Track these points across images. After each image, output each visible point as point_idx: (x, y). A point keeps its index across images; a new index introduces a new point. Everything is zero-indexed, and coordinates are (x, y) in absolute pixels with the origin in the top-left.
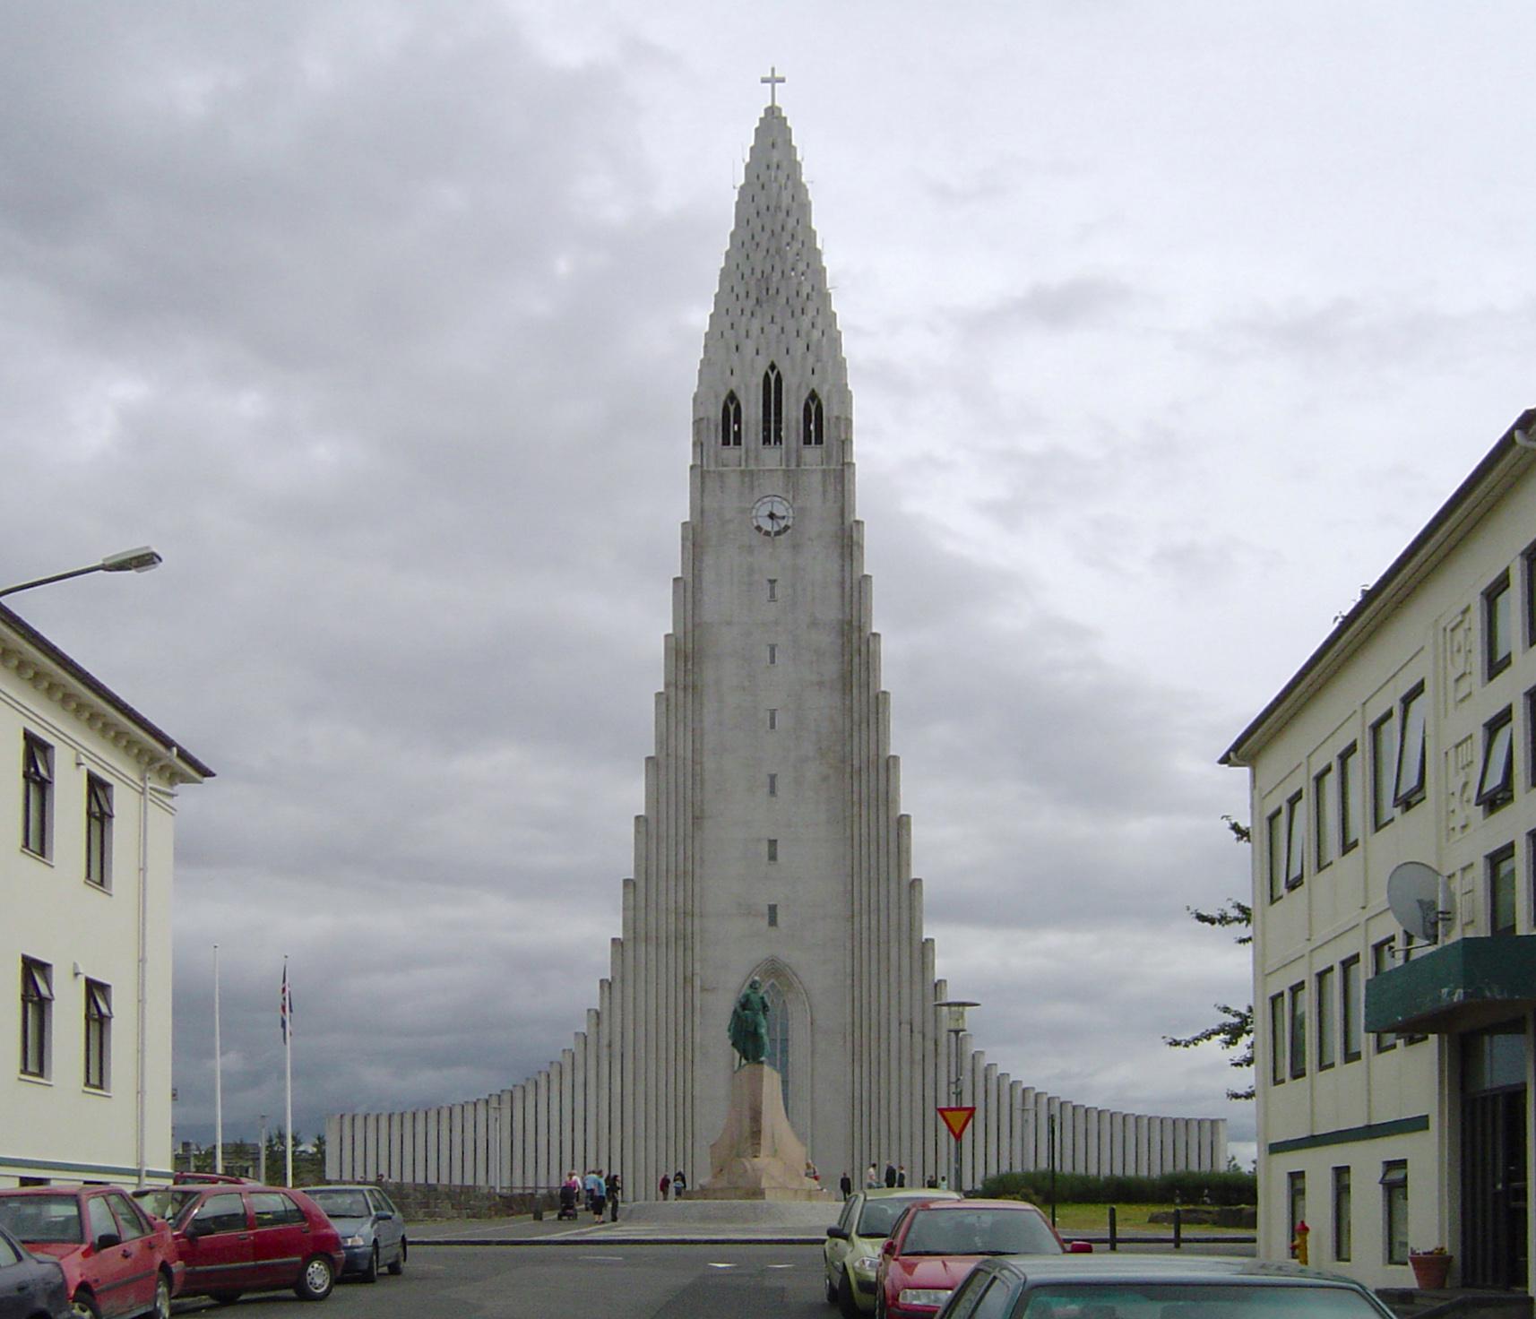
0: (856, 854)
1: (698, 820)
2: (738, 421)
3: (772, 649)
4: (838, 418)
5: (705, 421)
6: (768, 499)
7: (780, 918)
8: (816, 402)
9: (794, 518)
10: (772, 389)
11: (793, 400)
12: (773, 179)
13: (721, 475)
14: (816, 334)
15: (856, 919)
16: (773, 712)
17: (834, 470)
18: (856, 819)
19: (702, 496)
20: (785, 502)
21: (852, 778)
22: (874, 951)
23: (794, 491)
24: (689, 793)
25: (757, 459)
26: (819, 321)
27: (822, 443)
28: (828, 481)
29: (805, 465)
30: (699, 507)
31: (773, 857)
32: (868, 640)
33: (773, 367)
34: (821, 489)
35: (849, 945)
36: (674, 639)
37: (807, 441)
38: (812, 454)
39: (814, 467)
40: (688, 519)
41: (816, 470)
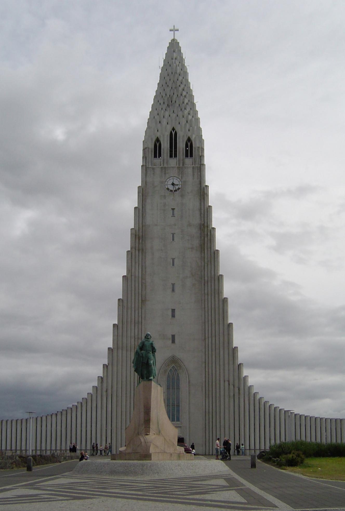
0: (206, 314)
1: (144, 301)
3: (173, 234)
4: (199, 147)
5: (147, 149)
6: (172, 178)
7: (177, 340)
8: (190, 142)
9: (181, 185)
10: (173, 138)
11: (181, 140)
12: (174, 62)
13: (153, 169)
14: (190, 117)
15: (207, 340)
16: (173, 260)
17: (197, 167)
18: (206, 301)
19: (146, 177)
20: (178, 179)
21: (205, 285)
22: (214, 353)
23: (182, 175)
24: (140, 291)
25: (167, 163)
26: (191, 112)
27: (192, 157)
29: (186, 165)
30: (145, 181)
31: (173, 316)
32: (211, 230)
33: (173, 129)
35: (203, 350)
36: (134, 230)
37: (187, 156)
38: (189, 161)
39: (189, 166)
40: (140, 185)
41: (190, 167)
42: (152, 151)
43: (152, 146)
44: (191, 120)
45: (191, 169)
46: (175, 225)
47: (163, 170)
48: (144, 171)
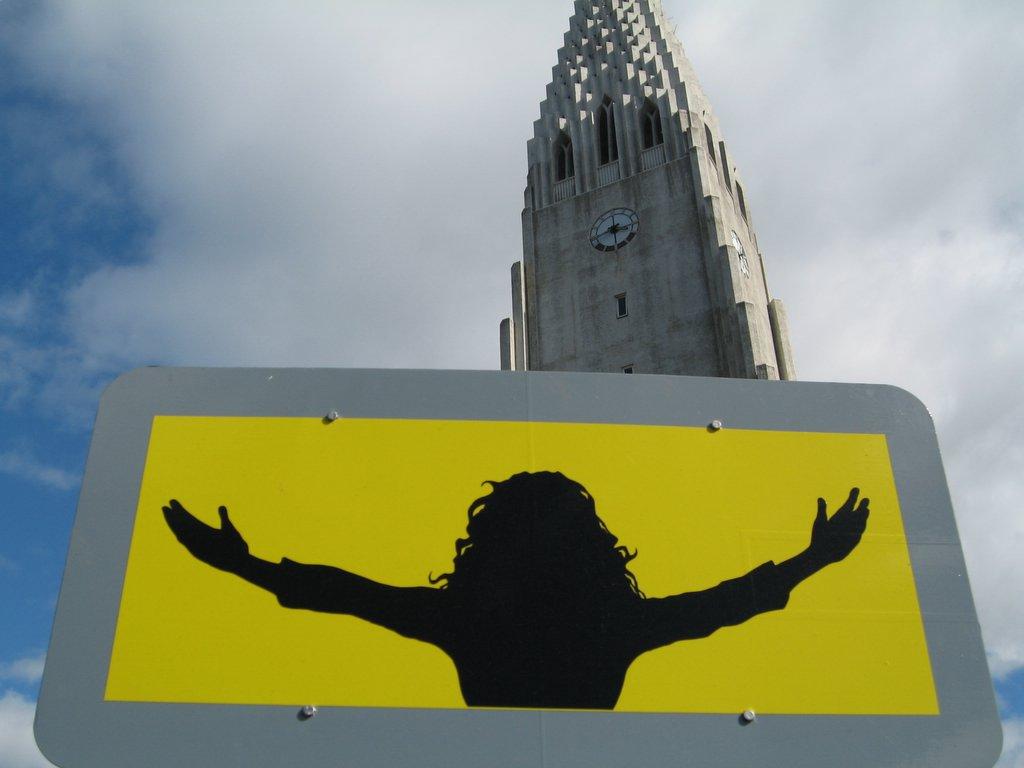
6: (608, 215)
13: (554, 210)
20: (627, 212)
28: (673, 173)
34: (666, 184)
38: (652, 157)
42: (548, 169)
43: (548, 156)
45: (663, 172)
46: (630, 339)
47: (582, 204)
48: (531, 224)
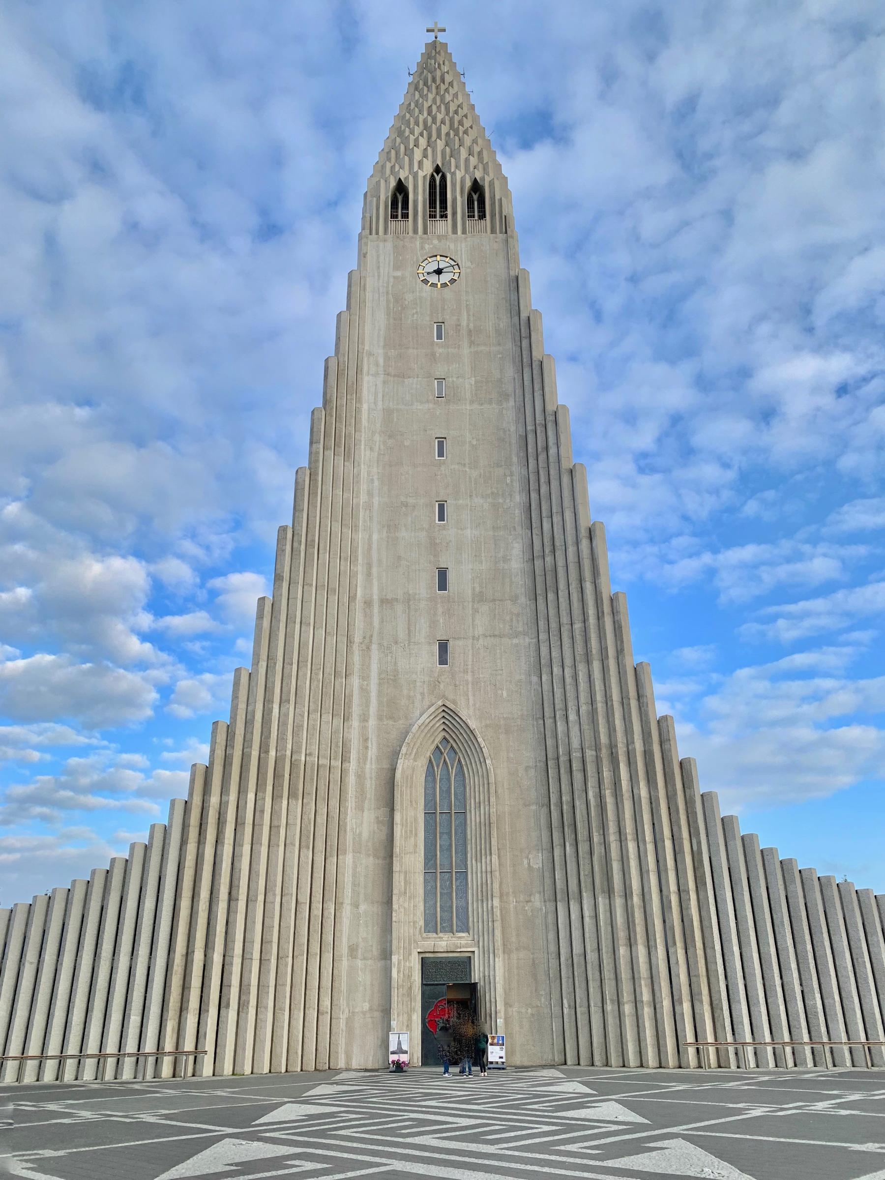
2: (405, 205)
6: (434, 259)
8: (477, 194)
44: (480, 153)
